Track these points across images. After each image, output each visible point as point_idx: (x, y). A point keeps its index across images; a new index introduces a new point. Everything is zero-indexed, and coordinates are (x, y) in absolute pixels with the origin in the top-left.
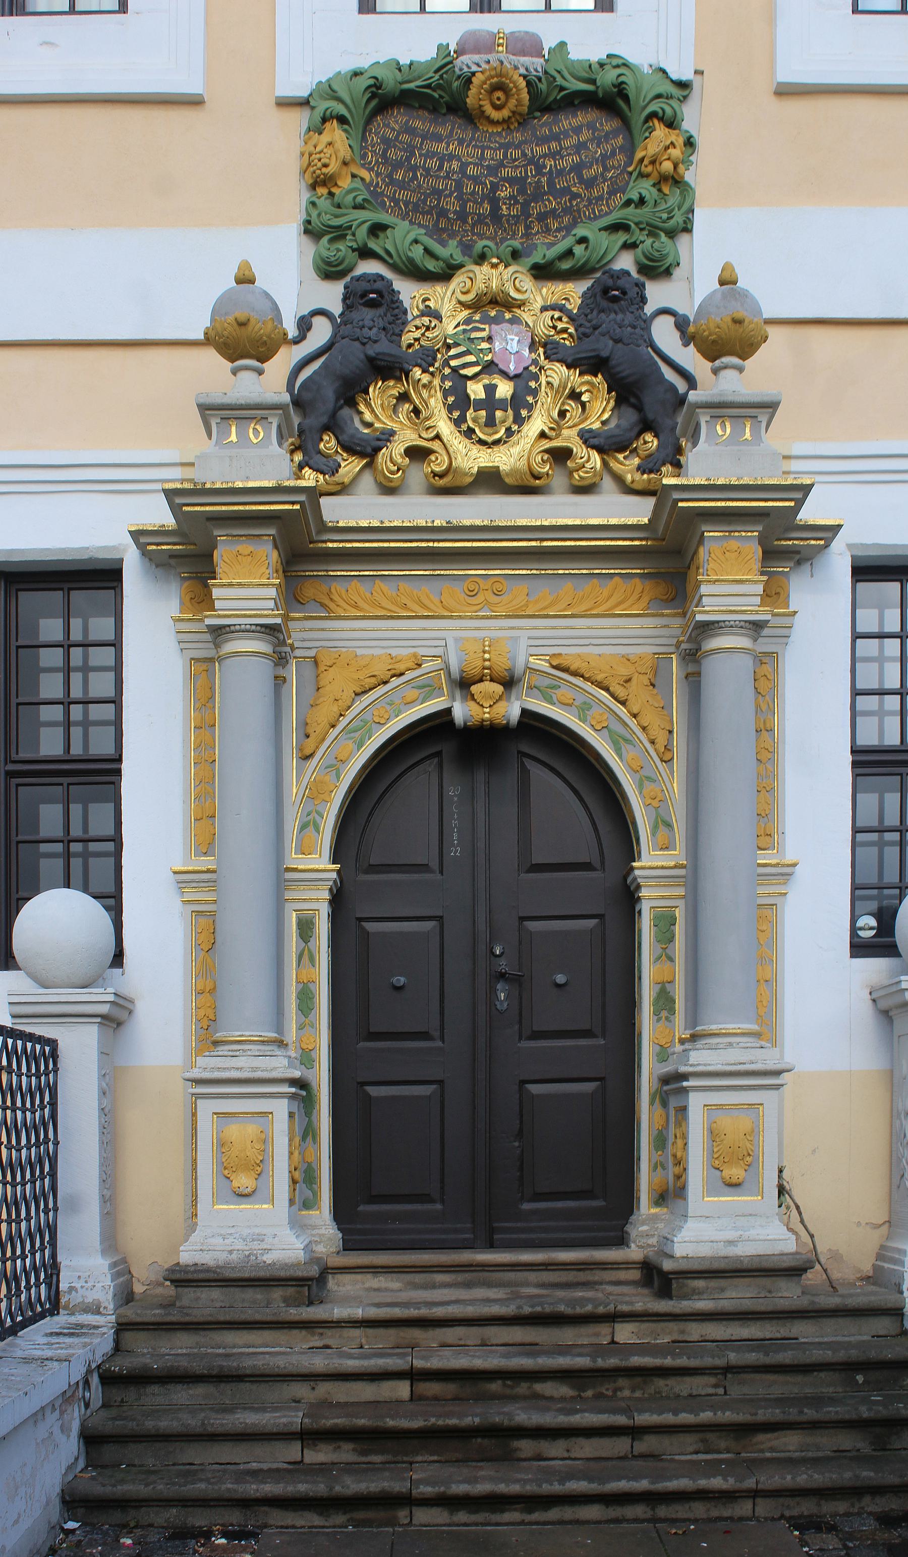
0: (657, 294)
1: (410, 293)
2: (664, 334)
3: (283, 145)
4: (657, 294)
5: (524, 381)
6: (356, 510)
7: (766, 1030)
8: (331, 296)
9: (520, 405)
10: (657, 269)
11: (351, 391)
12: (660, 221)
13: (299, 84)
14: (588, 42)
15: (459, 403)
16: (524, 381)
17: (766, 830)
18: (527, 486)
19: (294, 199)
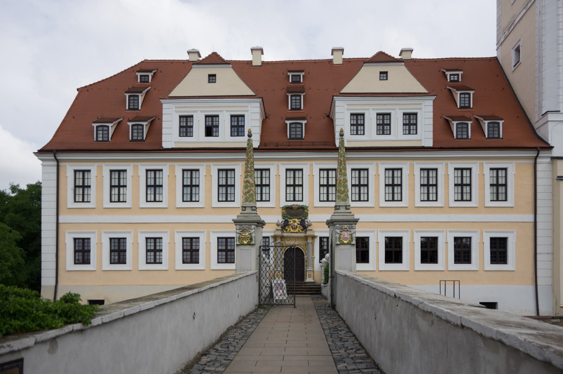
0: (306, 220)
1: (289, 220)
2: (306, 223)
3: (280, 210)
4: (306, 220)
5: (297, 226)
6: (285, 234)
7: (313, 267)
8: (284, 220)
9: (296, 228)
10: (306, 218)
11: (285, 227)
12: (306, 215)
13: (282, 206)
14: (300, 204)
15: (292, 228)
16: (297, 226)
17: (313, 255)
18: (297, 233)
19: (281, 214)
